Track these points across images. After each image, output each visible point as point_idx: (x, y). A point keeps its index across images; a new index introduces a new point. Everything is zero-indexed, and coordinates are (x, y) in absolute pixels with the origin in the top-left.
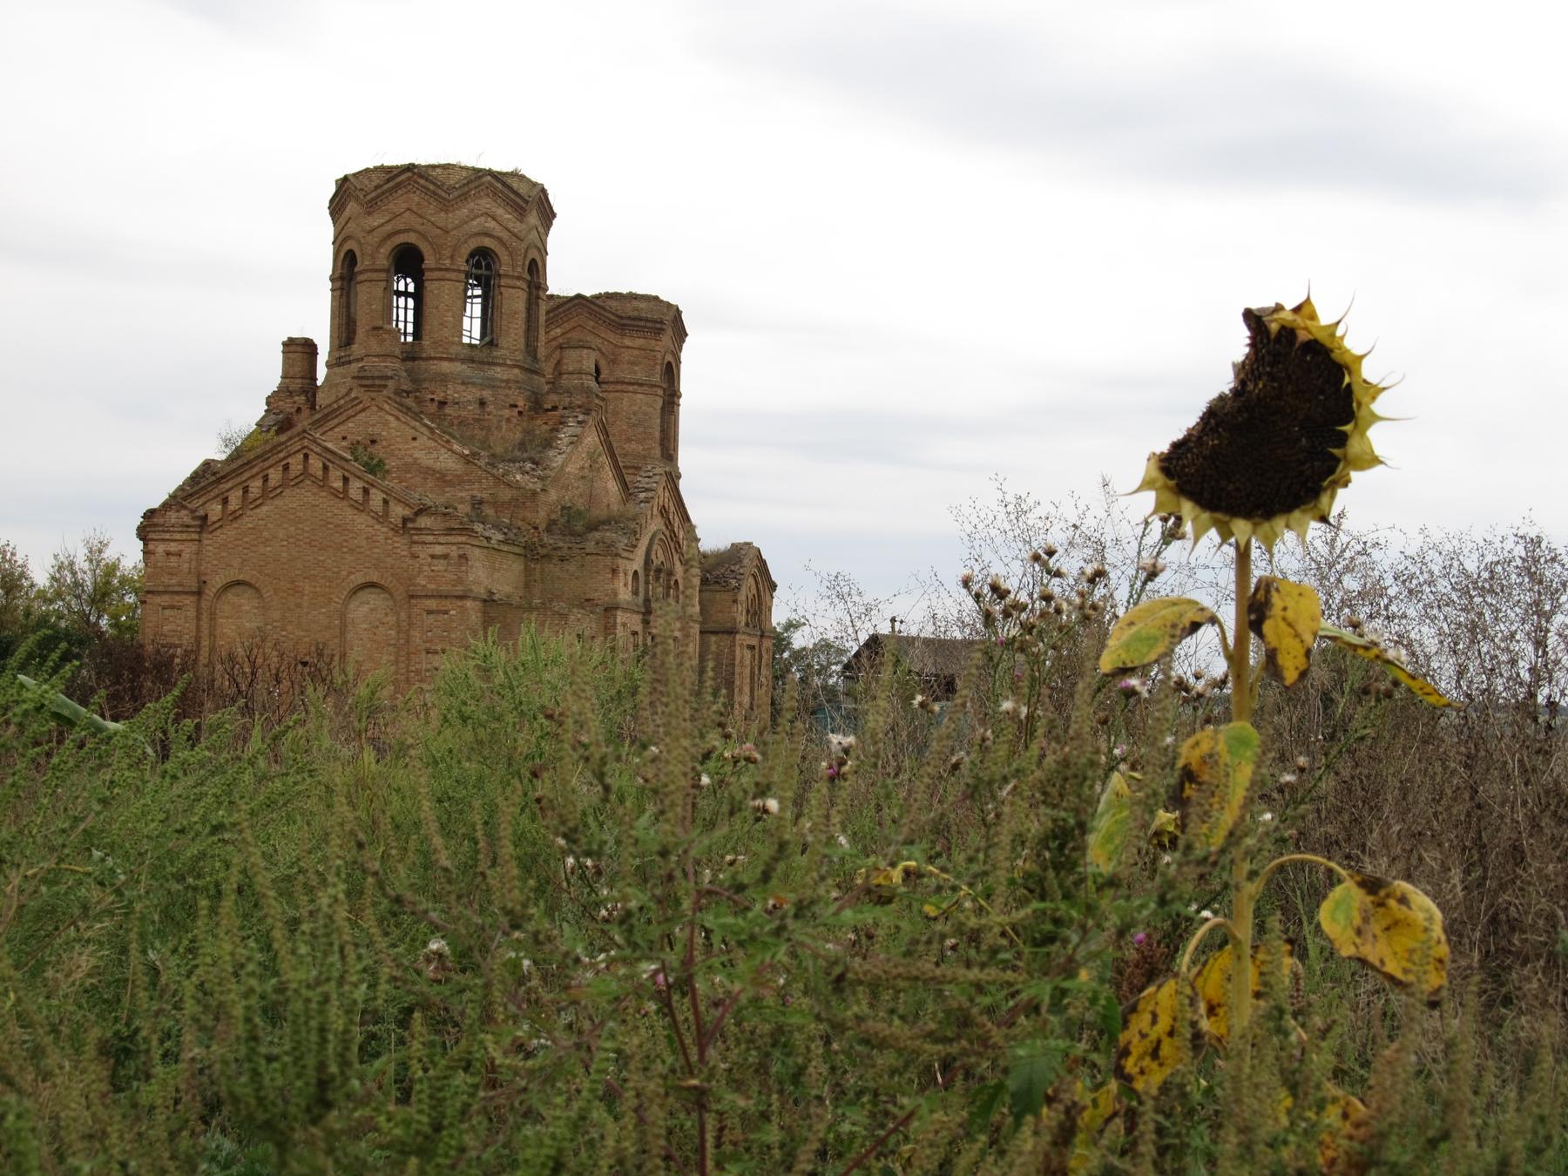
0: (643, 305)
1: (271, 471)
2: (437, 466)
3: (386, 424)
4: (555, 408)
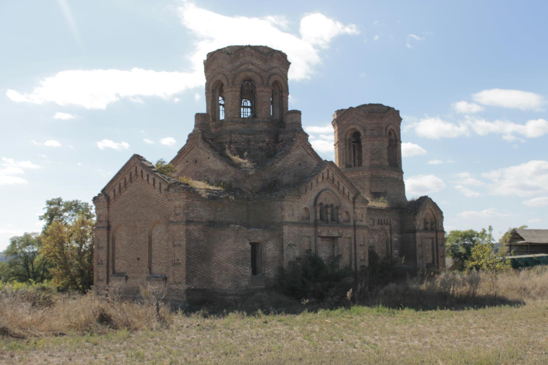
1: (126, 175)
4: (282, 141)
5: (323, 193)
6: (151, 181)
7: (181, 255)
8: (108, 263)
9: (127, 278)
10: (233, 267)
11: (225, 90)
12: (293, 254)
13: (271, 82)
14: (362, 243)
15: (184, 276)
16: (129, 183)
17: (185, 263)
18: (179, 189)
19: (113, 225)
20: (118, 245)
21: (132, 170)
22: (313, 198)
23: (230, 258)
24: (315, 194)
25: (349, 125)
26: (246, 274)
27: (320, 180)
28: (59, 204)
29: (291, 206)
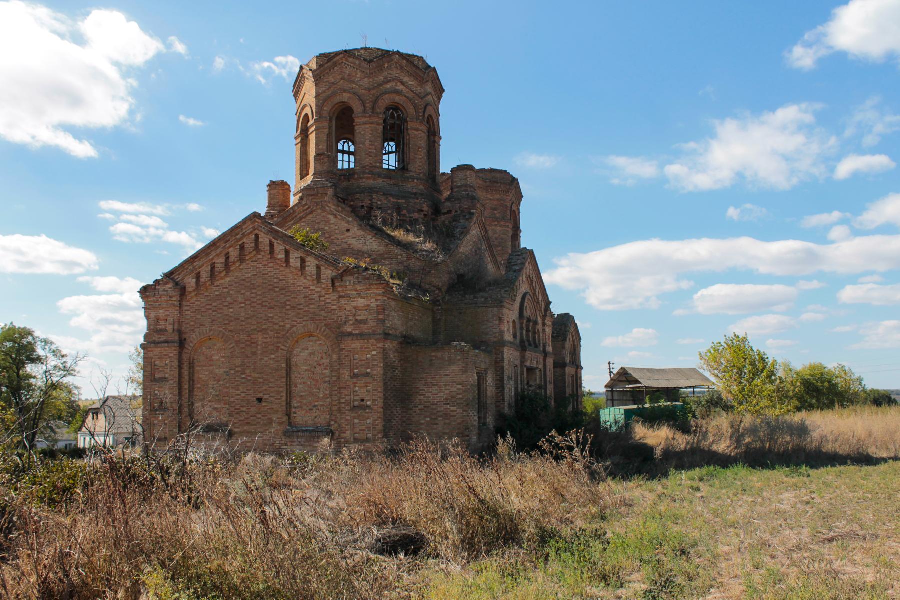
0: (498, 175)
1: (231, 250)
2: (365, 249)
3: (328, 222)
4: (450, 212)
6: (295, 261)
7: (371, 393)
11: (356, 120)
15: (380, 427)
19: (193, 338)
20: (202, 374)
21: (245, 240)
23: (453, 397)
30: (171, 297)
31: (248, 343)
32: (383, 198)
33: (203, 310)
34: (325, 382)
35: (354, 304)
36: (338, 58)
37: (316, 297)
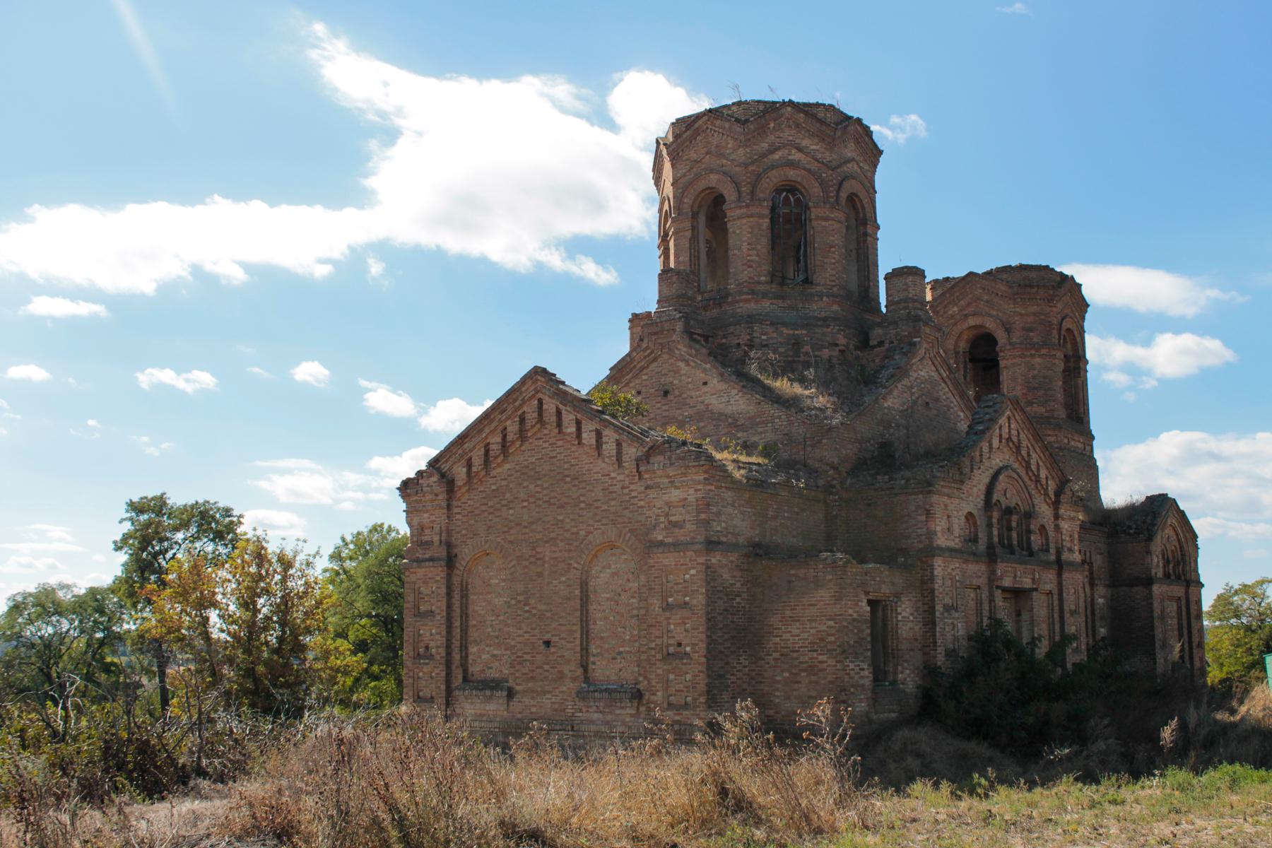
0: (1034, 275)
1: (509, 423)
3: (677, 371)
4: (881, 344)
5: (1001, 478)
6: (588, 437)
7: (689, 633)
8: (449, 654)
9: (511, 694)
10: (832, 662)
11: (729, 214)
12: (955, 629)
13: (844, 195)
14: (1073, 607)
15: (702, 686)
16: (518, 444)
17: (703, 652)
18: (683, 459)
19: (465, 553)
20: (478, 605)
21: (525, 409)
22: (983, 487)
23: (822, 640)
24: (985, 480)
25: (966, 316)
26: (862, 682)
27: (996, 443)
28: (159, 513)
29: (946, 506)
30: (436, 495)
31: (532, 559)
32: (769, 329)
33: (477, 512)
34: (633, 617)
35: (666, 498)
36: (700, 122)
37: (617, 488)
